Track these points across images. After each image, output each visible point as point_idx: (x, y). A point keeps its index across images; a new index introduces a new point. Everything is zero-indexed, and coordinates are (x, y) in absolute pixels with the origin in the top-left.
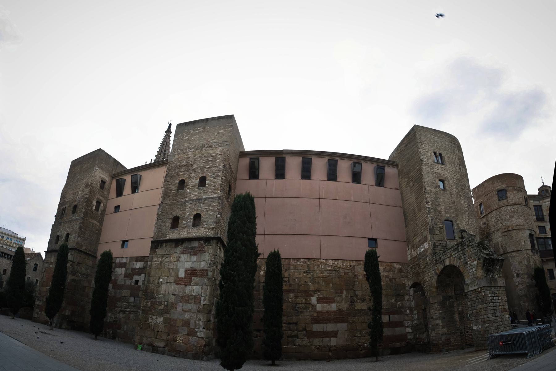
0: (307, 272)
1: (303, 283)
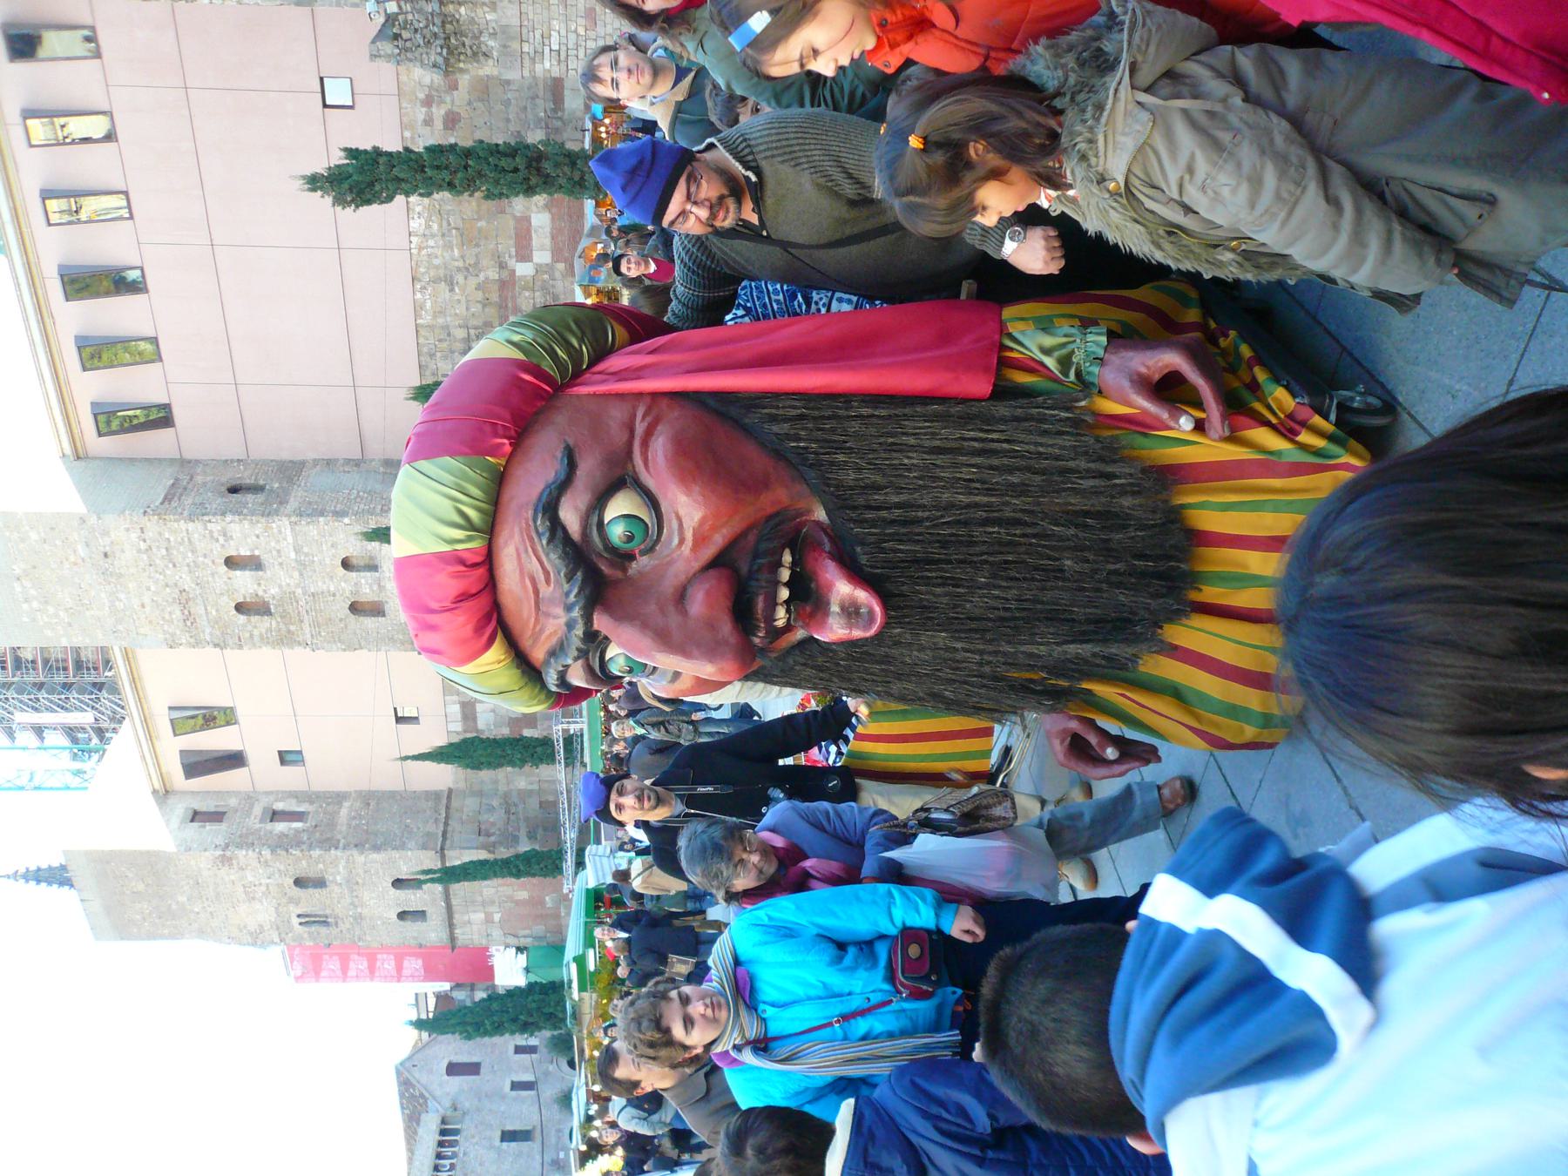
0: (451, 285)
1: (479, 295)
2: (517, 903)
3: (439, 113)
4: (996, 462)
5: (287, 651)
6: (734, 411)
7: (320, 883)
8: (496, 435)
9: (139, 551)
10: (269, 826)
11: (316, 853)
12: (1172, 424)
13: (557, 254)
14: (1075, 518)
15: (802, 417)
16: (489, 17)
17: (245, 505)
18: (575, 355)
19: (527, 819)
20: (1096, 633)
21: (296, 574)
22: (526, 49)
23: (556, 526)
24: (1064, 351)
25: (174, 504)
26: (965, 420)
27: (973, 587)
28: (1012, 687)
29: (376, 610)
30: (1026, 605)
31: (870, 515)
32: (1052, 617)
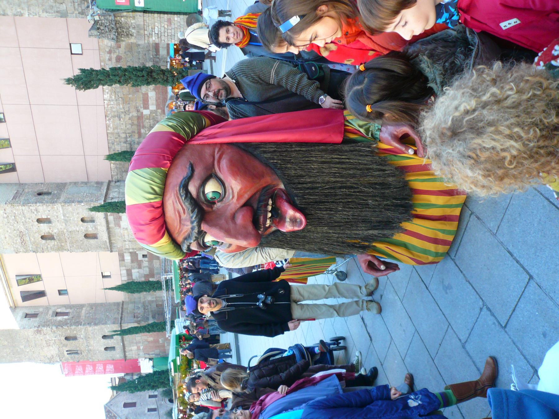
1: (130, 122)
2: (149, 342)
3: (114, 56)
4: (344, 166)
5: (61, 253)
6: (250, 150)
7: (75, 338)
8: (165, 160)
9: (4, 218)
10: (55, 318)
11: (73, 327)
12: (406, 152)
13: (158, 106)
14: (372, 185)
15: (275, 151)
16: (132, 22)
17: (44, 199)
18: (192, 130)
19: (152, 311)
20: (379, 226)
21: (64, 224)
22: (146, 33)
23: (187, 192)
24: (367, 127)
25: (17, 200)
26: (333, 152)
27: (337, 211)
28: (349, 246)
29: (94, 237)
30: (355, 217)
31: (300, 186)
32: (364, 221)
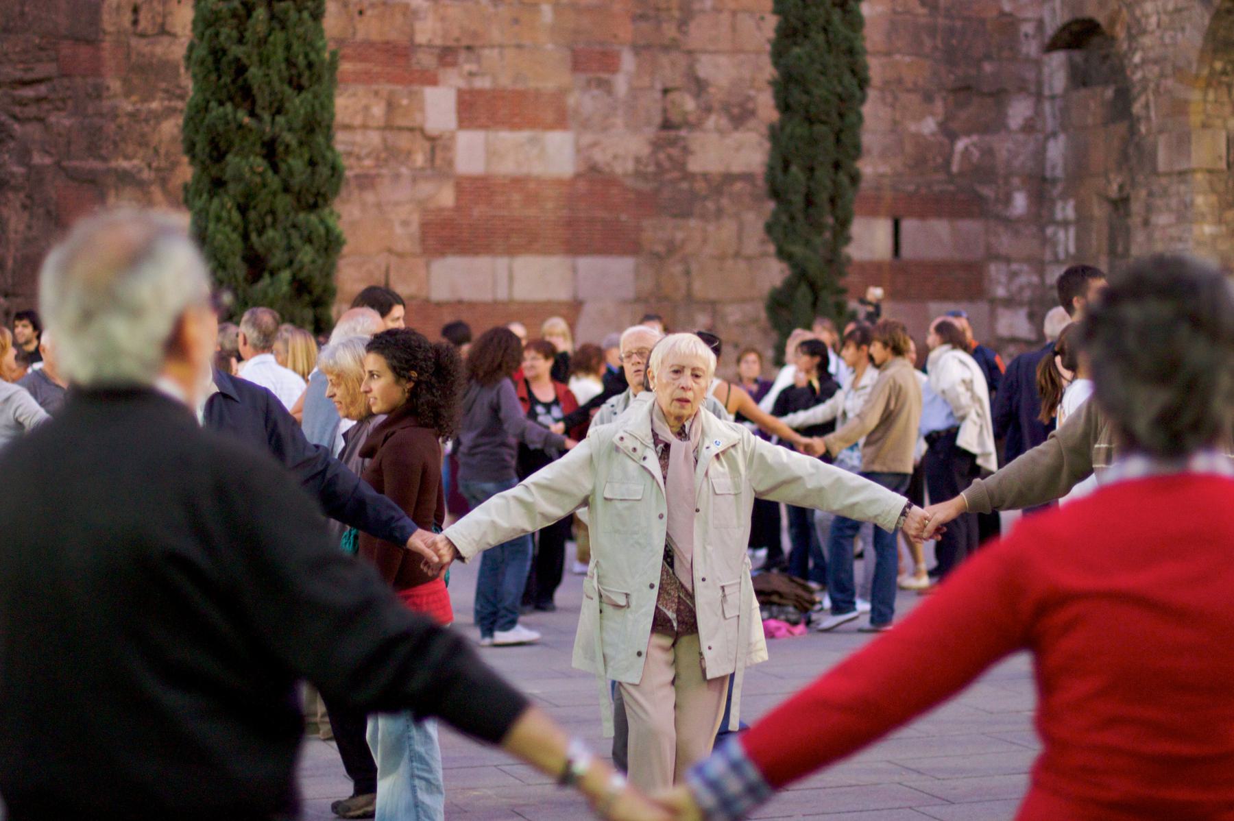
13: (477, 189)
